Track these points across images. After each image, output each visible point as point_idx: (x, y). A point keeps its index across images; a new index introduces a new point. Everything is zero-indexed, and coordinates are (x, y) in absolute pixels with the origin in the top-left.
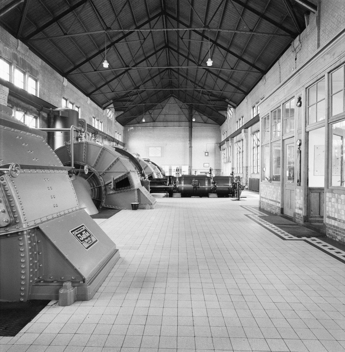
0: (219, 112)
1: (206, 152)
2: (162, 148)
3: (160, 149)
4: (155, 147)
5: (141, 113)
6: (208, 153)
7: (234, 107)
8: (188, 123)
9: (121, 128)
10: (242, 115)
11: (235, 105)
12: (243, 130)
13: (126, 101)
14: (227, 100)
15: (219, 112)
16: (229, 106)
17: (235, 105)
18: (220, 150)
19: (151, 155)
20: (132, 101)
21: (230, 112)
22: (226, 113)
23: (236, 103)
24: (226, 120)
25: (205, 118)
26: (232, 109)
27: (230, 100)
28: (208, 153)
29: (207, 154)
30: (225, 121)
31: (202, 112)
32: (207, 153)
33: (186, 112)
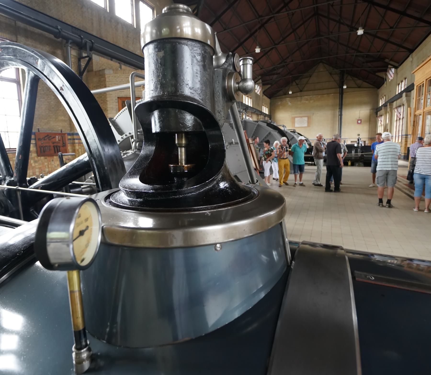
0: (377, 74)
1: (358, 120)
2: (309, 118)
3: (306, 119)
4: (301, 117)
5: (287, 84)
6: (361, 120)
7: (396, 68)
8: (338, 89)
9: (268, 100)
10: (404, 76)
11: (397, 65)
12: (404, 94)
13: (274, 74)
14: (387, 60)
15: (377, 74)
16: (390, 66)
17: (397, 65)
18: (377, 117)
19: (297, 125)
20: (279, 74)
21: (391, 74)
22: (386, 75)
23: (398, 63)
24: (385, 83)
25: (359, 82)
26: (393, 70)
27: (391, 60)
28: (361, 120)
29: (359, 122)
30: (384, 83)
31: (355, 75)
32: (359, 121)
33: (337, 78)
